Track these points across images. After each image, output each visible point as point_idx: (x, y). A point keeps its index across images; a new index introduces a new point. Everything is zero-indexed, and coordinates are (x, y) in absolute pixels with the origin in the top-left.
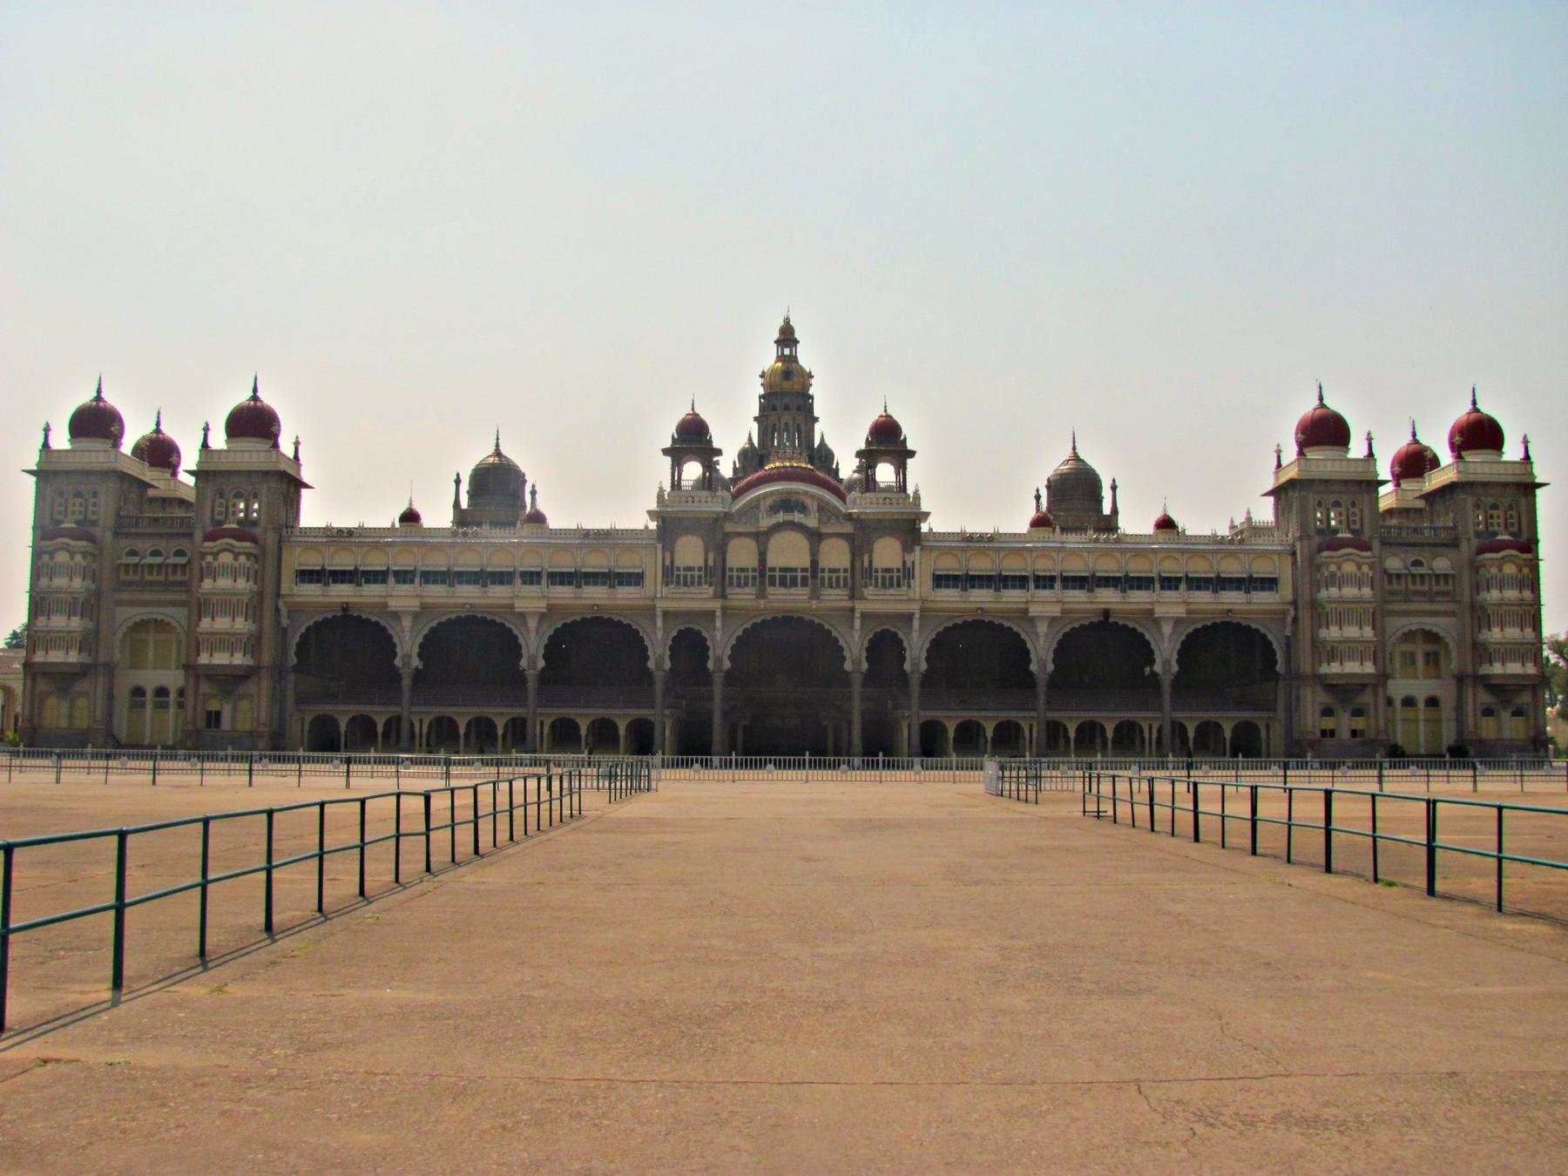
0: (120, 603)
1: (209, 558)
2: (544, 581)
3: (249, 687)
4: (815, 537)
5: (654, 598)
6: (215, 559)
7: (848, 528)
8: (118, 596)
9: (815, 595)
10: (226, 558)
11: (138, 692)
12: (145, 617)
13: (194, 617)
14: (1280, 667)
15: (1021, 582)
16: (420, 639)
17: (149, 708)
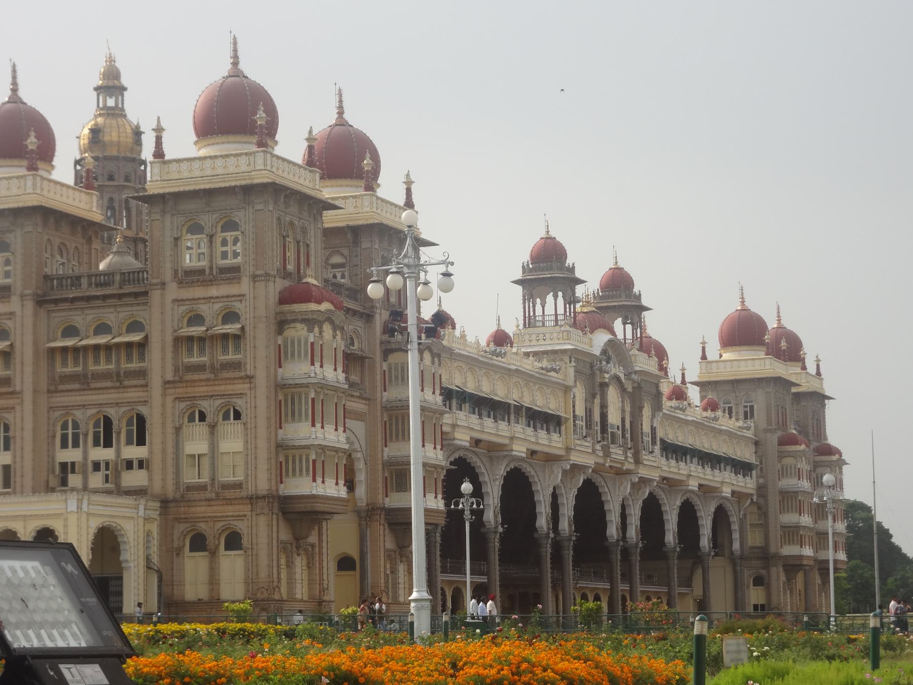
2: (523, 420)
4: (623, 390)
5: (568, 449)
7: (630, 389)
14: (736, 546)
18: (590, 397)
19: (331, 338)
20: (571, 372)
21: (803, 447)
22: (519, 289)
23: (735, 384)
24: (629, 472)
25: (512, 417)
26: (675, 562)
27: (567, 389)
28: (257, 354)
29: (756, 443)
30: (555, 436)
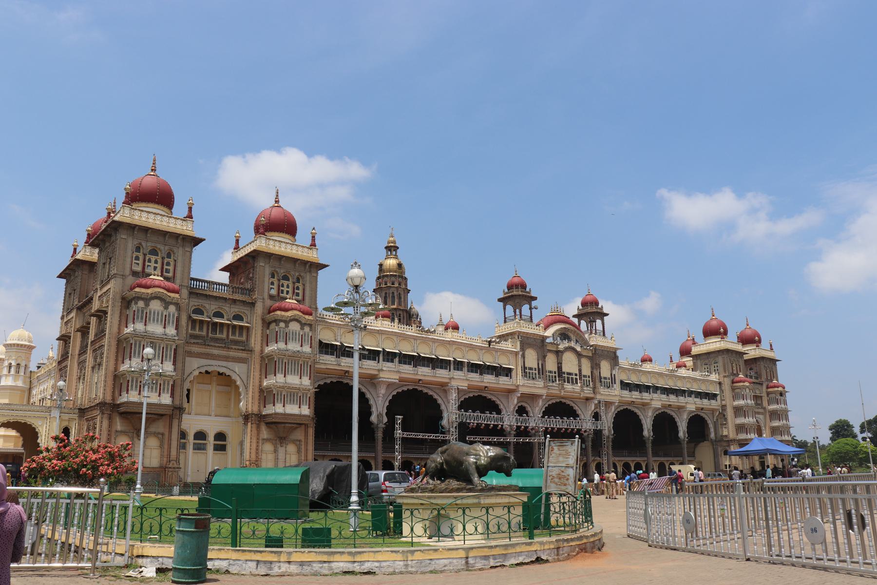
0: (191, 354)
1: (282, 325)
2: (465, 369)
3: (299, 435)
4: (579, 355)
6: (287, 326)
7: (590, 355)
8: (188, 348)
9: (582, 390)
10: (294, 327)
11: (183, 435)
12: (210, 369)
13: (257, 374)
14: (712, 435)
15: (647, 388)
16: (387, 404)
17: (190, 447)
18: (542, 357)
19: (162, 308)
20: (519, 343)
21: (747, 384)
22: (502, 304)
23: (708, 354)
24: (592, 398)
25: (452, 367)
26: (649, 446)
27: (516, 353)
28: (112, 321)
29: (720, 383)
30: (505, 378)
